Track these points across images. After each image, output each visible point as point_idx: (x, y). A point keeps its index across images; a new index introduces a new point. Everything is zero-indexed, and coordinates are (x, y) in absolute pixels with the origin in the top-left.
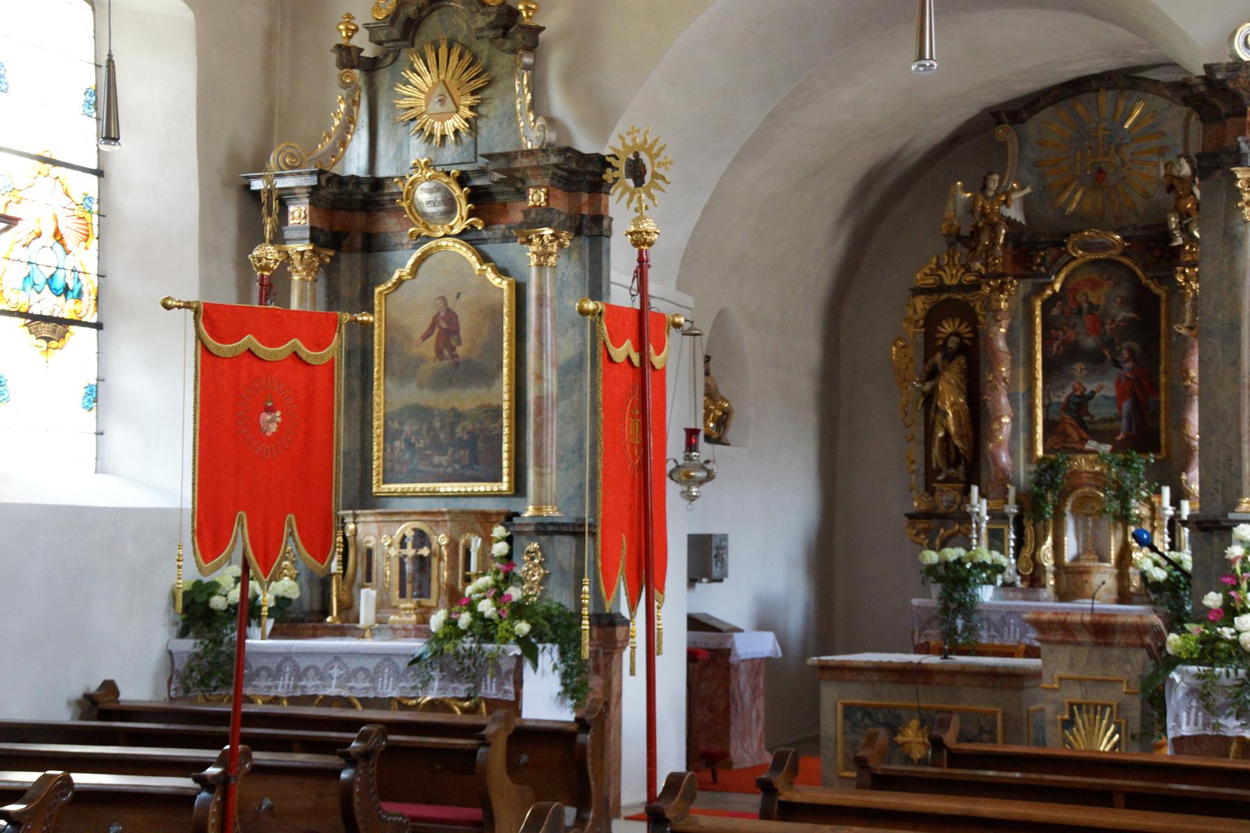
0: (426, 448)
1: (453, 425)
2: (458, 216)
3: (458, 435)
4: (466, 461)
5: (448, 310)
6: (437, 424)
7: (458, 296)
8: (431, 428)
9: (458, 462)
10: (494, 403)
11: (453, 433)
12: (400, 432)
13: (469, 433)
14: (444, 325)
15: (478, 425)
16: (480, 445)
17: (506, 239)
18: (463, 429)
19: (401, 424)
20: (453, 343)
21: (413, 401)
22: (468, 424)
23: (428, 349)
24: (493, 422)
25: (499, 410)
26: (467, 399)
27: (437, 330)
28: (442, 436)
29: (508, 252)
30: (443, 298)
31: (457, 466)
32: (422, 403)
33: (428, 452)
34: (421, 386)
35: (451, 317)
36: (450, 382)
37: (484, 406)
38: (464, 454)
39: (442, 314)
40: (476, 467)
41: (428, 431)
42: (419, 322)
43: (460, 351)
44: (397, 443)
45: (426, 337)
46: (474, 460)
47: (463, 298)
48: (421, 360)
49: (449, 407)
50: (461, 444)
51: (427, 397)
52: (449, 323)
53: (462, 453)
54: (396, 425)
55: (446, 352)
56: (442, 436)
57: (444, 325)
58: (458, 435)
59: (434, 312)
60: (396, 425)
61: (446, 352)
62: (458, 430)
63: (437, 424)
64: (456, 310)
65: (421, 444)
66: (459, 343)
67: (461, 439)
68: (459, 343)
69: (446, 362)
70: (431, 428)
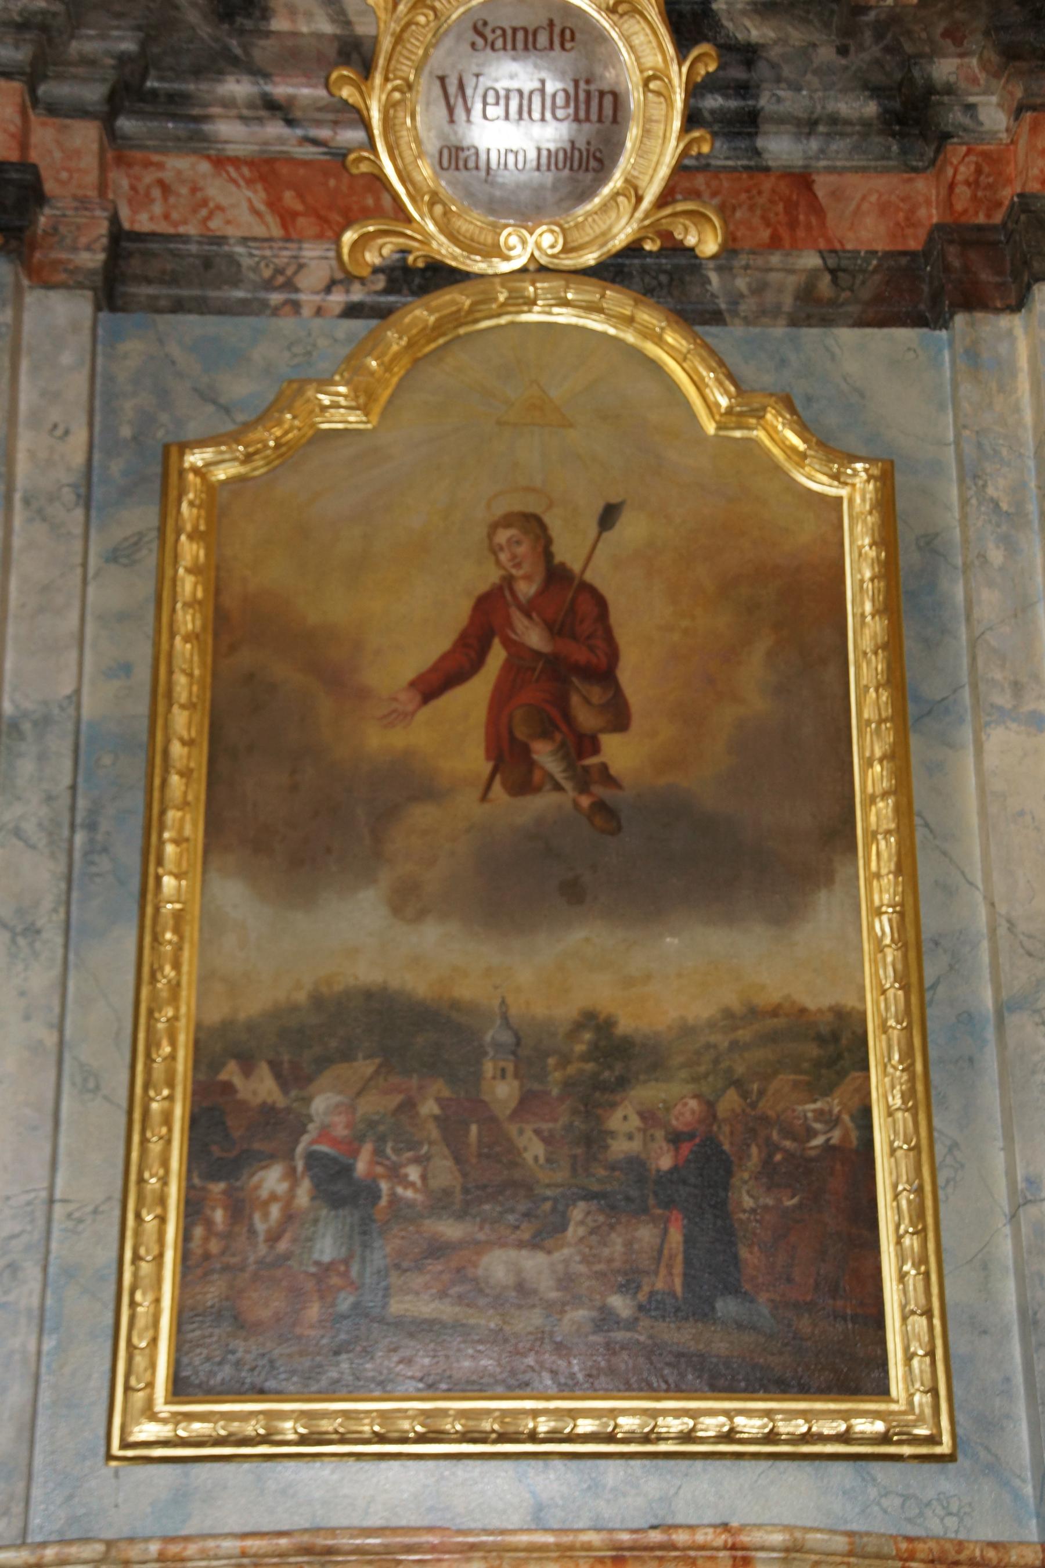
0: (440, 1203)
1: (595, 1095)
2: (616, 181)
3: (620, 1148)
4: (671, 1280)
5: (556, 576)
6: (503, 1092)
7: (609, 516)
8: (465, 1111)
9: (629, 1284)
10: (817, 997)
11: (594, 1140)
12: (279, 1126)
13: (676, 1139)
14: (534, 637)
15: (730, 1101)
16: (747, 1197)
17: (812, 309)
18: (648, 1117)
19: (294, 1078)
20: (586, 718)
21: (365, 974)
22: (679, 1099)
23: (456, 732)
24: (818, 1088)
25: (836, 1048)
26: (679, 975)
27: (497, 656)
28: (534, 1150)
29: (862, 355)
30: (533, 525)
31: (620, 1304)
32: (418, 985)
33: (451, 1230)
34: (407, 902)
35: (575, 607)
36: (574, 893)
37: (753, 1013)
38: (660, 1240)
39: (526, 589)
40: (726, 1307)
41: (451, 1126)
42: (411, 620)
43: (619, 753)
44: (271, 1180)
45: (434, 685)
46: (714, 1269)
47: (631, 529)
48: (408, 784)
49: (566, 1011)
50: (631, 1195)
51: (436, 957)
52: (555, 629)
53: (646, 1234)
54: (261, 1088)
55: (546, 756)
56: (534, 1150)
57: (534, 637)
58: (620, 1148)
59: (493, 576)
60: (261, 1088)
61: (546, 756)
62: (623, 1121)
63: (503, 1092)
64: (600, 575)
65: (411, 1184)
66: (619, 718)
67: (636, 1165)
68: (619, 718)
69: (542, 802)
70: (465, 1111)
